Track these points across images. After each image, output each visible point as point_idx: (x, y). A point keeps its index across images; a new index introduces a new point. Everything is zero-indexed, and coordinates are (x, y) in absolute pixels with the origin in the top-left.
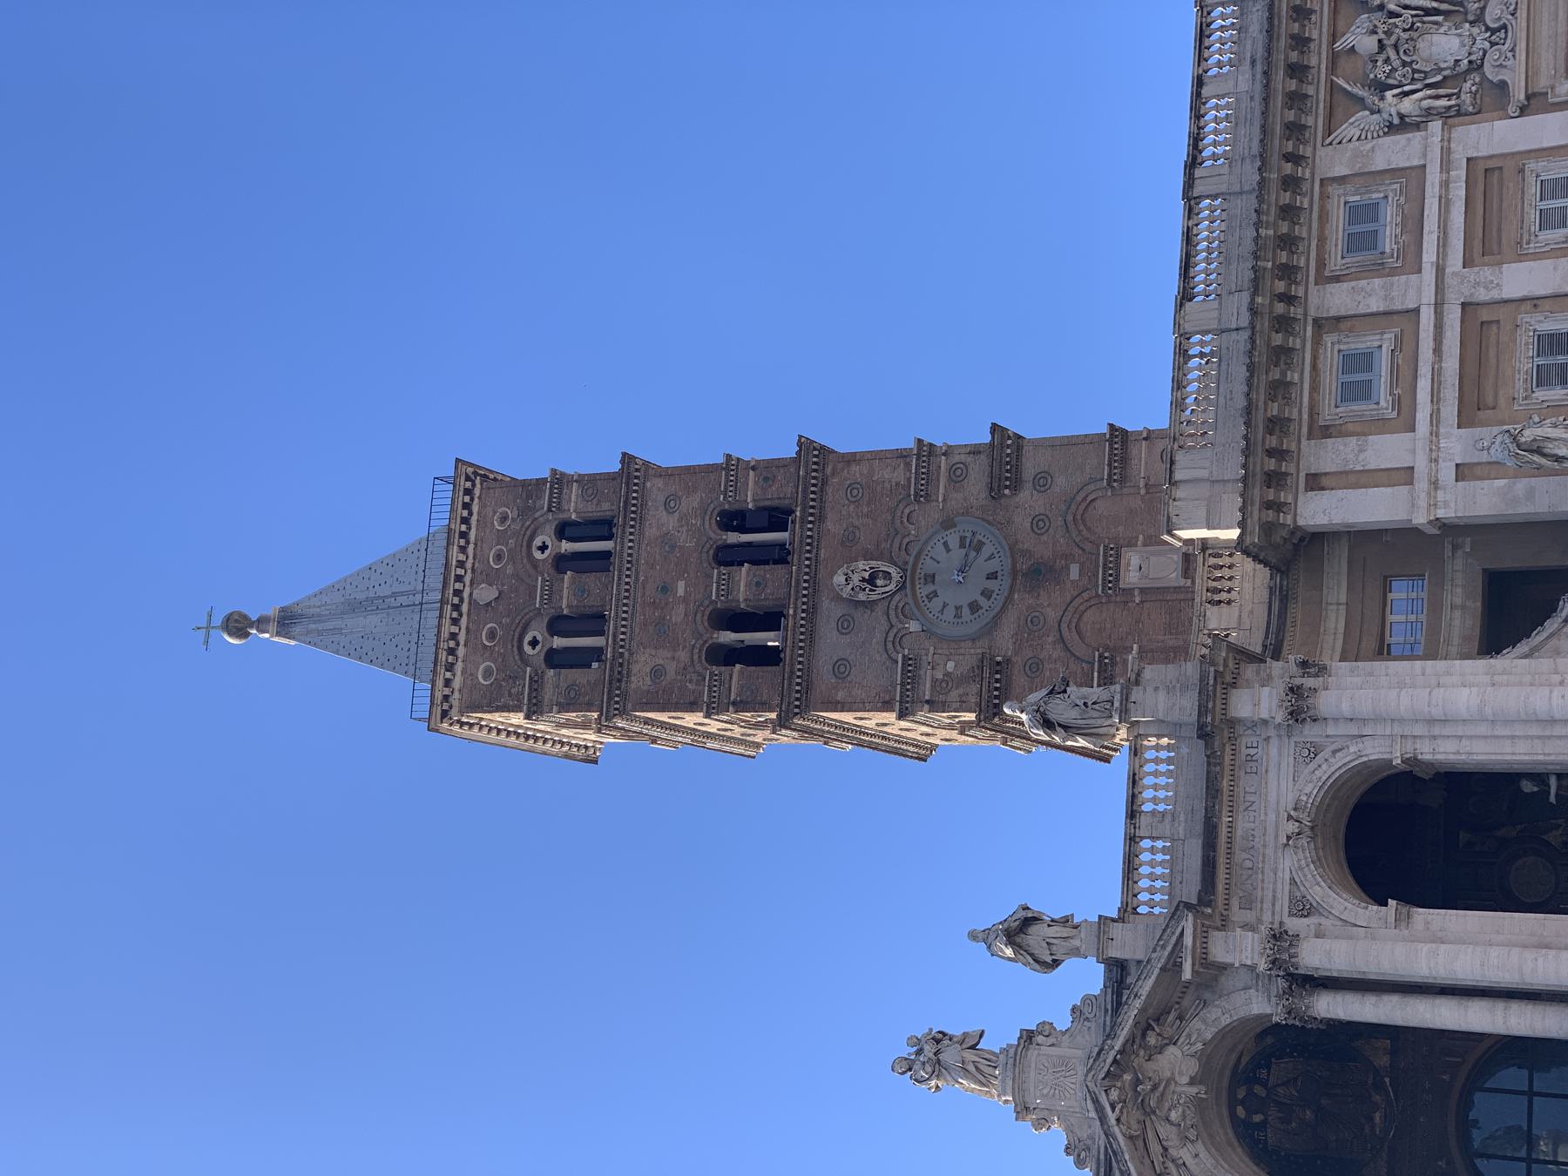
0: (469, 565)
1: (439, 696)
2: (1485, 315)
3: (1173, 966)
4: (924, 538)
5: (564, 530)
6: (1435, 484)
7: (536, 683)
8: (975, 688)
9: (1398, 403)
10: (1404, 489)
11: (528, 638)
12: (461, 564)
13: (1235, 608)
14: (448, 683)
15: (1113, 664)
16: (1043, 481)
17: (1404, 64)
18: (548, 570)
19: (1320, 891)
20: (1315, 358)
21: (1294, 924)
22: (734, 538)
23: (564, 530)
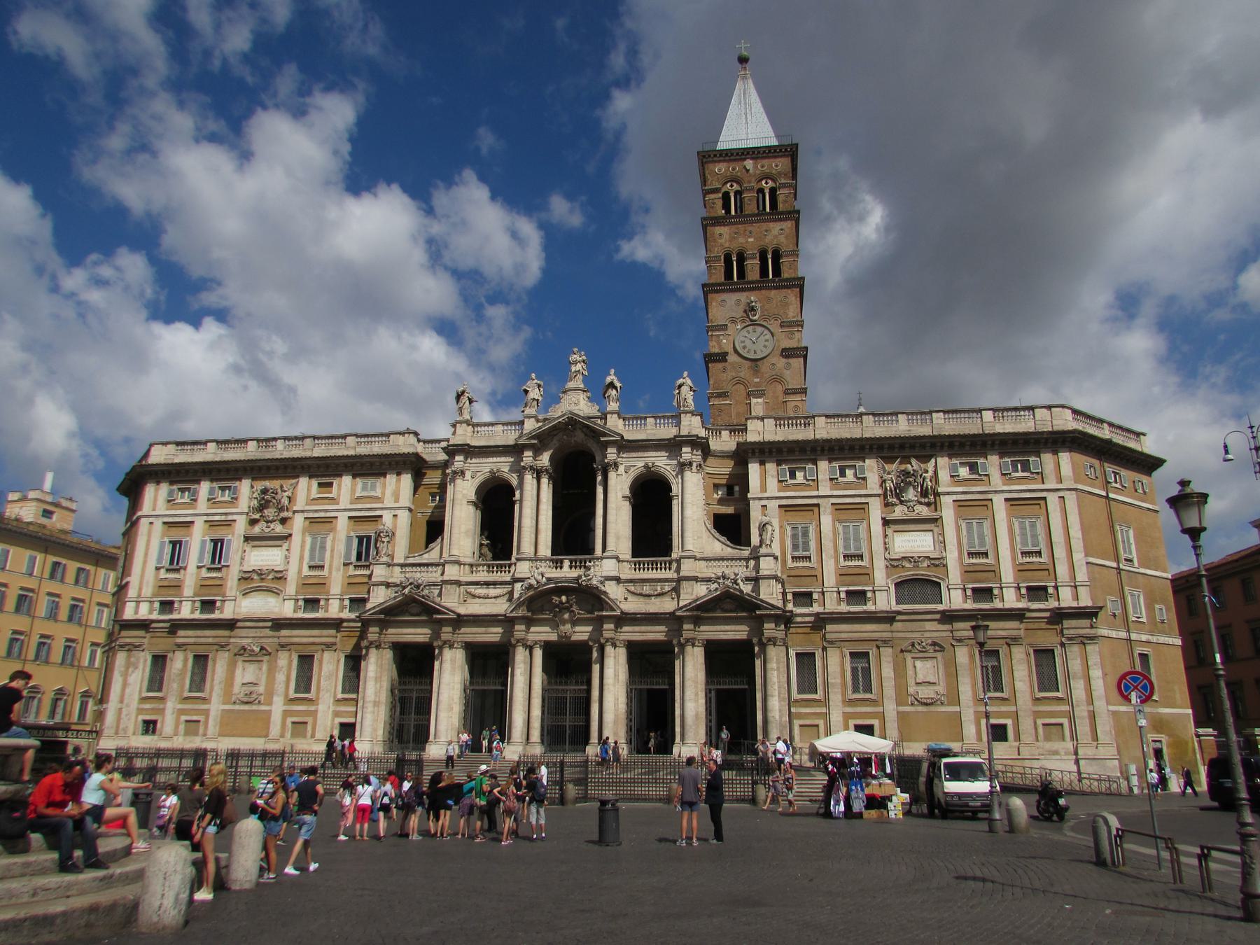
0: (760, 155)
1: (710, 153)
2: (816, 509)
3: (605, 435)
4: (769, 326)
5: (773, 191)
6: (760, 499)
7: (716, 191)
8: (716, 350)
9: (788, 486)
10: (759, 489)
11: (735, 185)
12: (759, 152)
13: (728, 439)
14: (715, 156)
15: (726, 396)
16: (788, 366)
17: (902, 481)
18: (757, 187)
19: (633, 474)
20: (804, 459)
21: (621, 469)
22: (770, 256)
23: (773, 191)
